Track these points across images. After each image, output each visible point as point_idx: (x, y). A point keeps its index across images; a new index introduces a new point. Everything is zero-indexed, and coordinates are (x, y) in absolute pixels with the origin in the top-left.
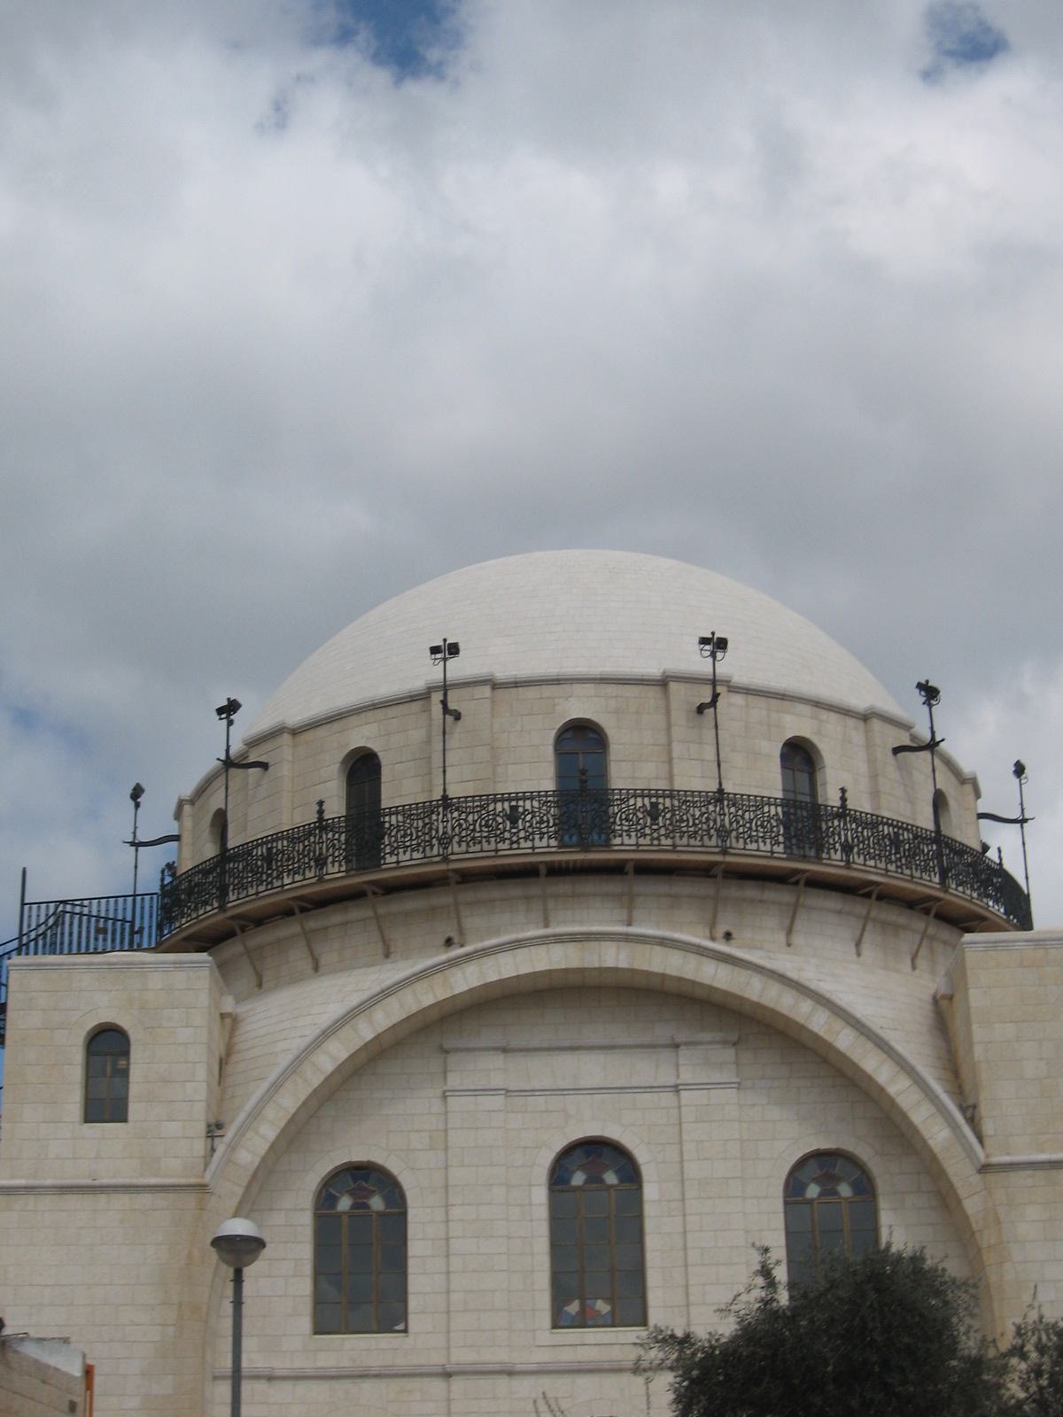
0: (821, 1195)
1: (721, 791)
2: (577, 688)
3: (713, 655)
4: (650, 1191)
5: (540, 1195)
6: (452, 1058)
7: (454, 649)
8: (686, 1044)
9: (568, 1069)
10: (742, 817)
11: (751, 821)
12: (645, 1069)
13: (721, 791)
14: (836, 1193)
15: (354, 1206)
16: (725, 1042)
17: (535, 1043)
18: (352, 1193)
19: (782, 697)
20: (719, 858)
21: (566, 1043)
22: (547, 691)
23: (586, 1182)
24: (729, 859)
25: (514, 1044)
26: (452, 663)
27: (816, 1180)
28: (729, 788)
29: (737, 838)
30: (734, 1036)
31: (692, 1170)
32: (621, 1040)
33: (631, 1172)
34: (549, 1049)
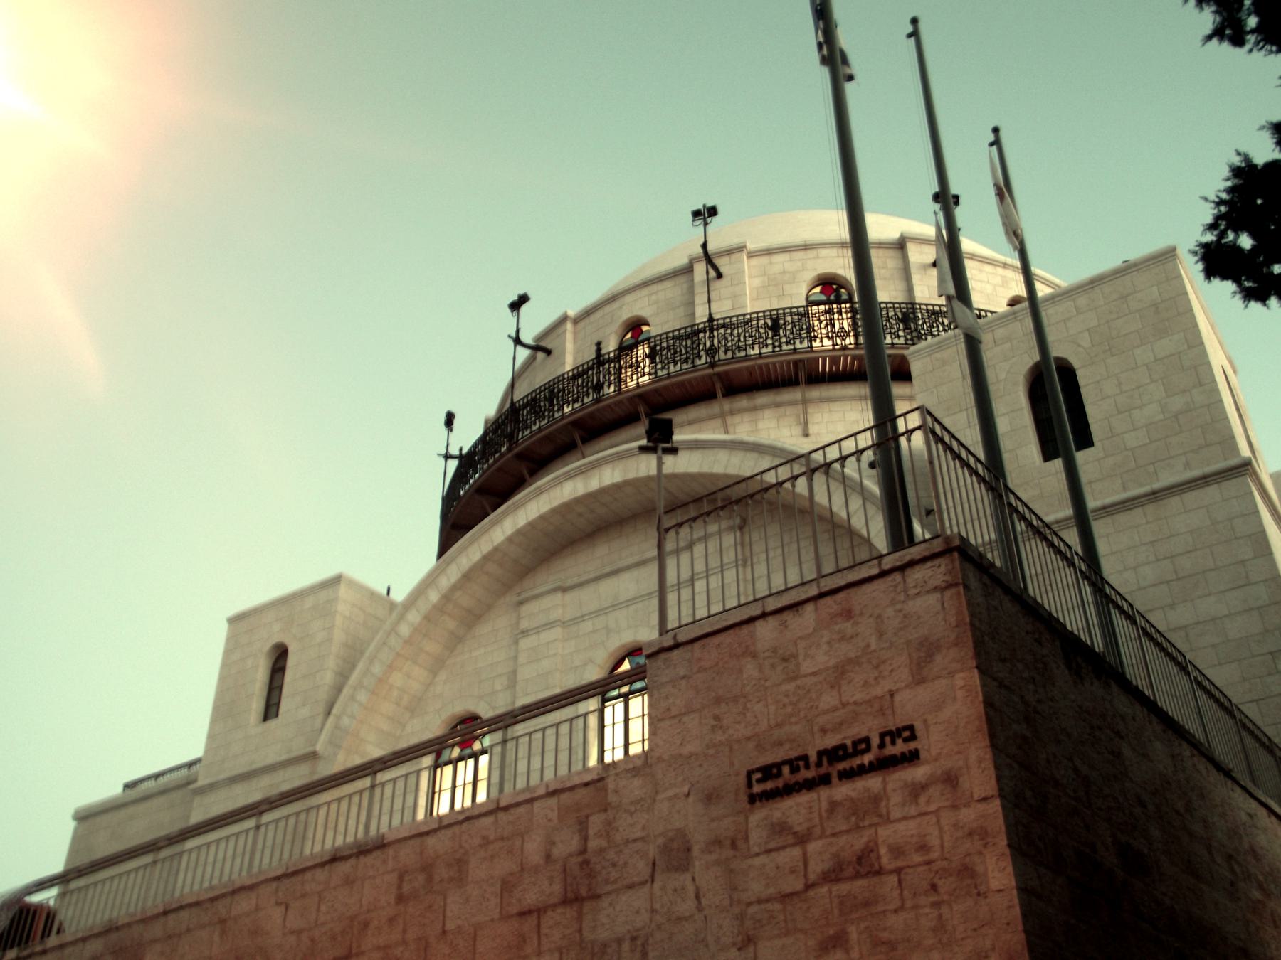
1: (711, 319)
2: (628, 298)
3: (706, 224)
10: (731, 334)
11: (739, 336)
13: (711, 319)
16: (731, 528)
19: (806, 247)
20: (710, 371)
21: (607, 570)
22: (608, 309)
24: (717, 370)
26: (524, 309)
28: (716, 316)
29: (726, 352)
30: (738, 521)
34: (597, 579)
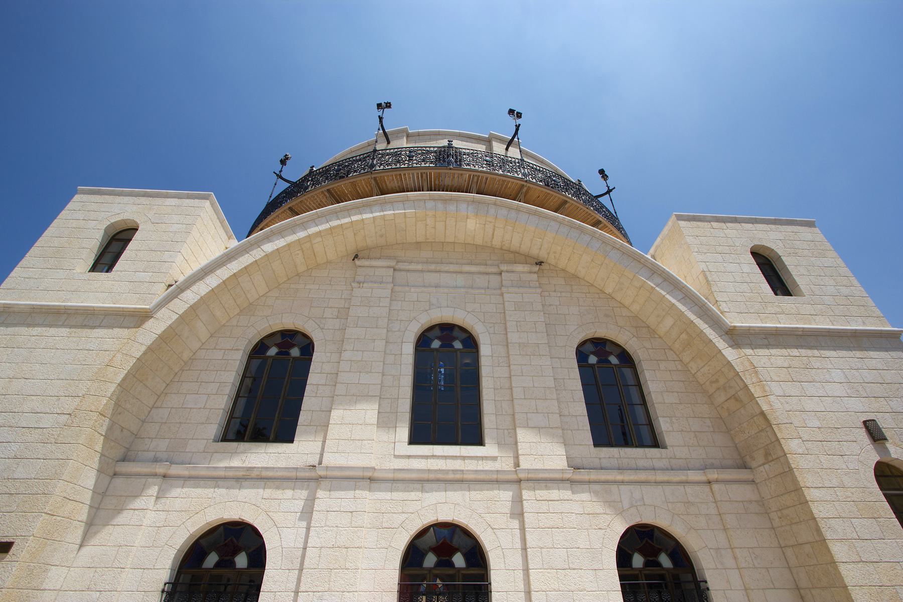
0: (598, 362)
4: (485, 350)
5: (409, 349)
6: (359, 270)
7: (388, 105)
8: (507, 271)
9: (432, 278)
12: (481, 281)
14: (609, 362)
15: (277, 354)
16: (530, 272)
17: (413, 267)
18: (278, 345)
21: (433, 267)
23: (441, 346)
25: (401, 266)
27: (594, 353)
31: (513, 337)
32: (467, 268)
33: (471, 343)
34: (422, 271)
